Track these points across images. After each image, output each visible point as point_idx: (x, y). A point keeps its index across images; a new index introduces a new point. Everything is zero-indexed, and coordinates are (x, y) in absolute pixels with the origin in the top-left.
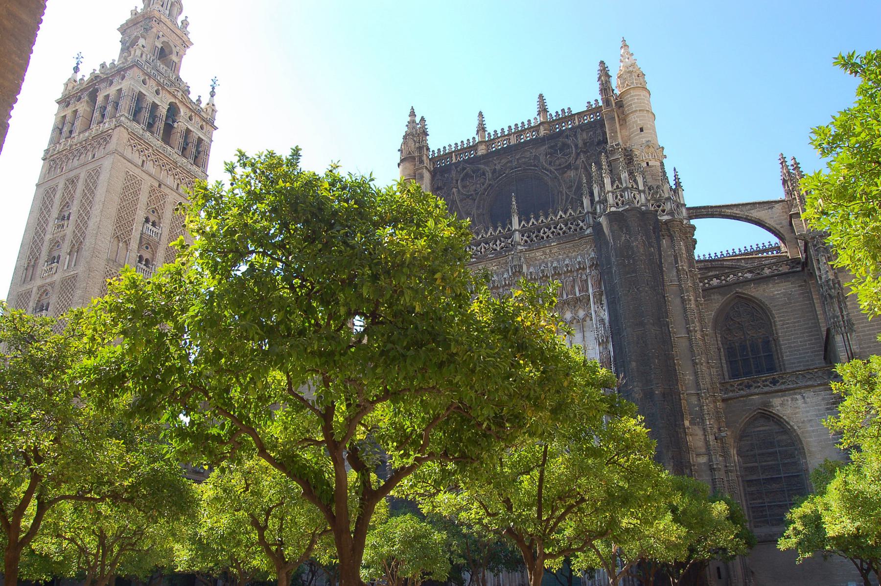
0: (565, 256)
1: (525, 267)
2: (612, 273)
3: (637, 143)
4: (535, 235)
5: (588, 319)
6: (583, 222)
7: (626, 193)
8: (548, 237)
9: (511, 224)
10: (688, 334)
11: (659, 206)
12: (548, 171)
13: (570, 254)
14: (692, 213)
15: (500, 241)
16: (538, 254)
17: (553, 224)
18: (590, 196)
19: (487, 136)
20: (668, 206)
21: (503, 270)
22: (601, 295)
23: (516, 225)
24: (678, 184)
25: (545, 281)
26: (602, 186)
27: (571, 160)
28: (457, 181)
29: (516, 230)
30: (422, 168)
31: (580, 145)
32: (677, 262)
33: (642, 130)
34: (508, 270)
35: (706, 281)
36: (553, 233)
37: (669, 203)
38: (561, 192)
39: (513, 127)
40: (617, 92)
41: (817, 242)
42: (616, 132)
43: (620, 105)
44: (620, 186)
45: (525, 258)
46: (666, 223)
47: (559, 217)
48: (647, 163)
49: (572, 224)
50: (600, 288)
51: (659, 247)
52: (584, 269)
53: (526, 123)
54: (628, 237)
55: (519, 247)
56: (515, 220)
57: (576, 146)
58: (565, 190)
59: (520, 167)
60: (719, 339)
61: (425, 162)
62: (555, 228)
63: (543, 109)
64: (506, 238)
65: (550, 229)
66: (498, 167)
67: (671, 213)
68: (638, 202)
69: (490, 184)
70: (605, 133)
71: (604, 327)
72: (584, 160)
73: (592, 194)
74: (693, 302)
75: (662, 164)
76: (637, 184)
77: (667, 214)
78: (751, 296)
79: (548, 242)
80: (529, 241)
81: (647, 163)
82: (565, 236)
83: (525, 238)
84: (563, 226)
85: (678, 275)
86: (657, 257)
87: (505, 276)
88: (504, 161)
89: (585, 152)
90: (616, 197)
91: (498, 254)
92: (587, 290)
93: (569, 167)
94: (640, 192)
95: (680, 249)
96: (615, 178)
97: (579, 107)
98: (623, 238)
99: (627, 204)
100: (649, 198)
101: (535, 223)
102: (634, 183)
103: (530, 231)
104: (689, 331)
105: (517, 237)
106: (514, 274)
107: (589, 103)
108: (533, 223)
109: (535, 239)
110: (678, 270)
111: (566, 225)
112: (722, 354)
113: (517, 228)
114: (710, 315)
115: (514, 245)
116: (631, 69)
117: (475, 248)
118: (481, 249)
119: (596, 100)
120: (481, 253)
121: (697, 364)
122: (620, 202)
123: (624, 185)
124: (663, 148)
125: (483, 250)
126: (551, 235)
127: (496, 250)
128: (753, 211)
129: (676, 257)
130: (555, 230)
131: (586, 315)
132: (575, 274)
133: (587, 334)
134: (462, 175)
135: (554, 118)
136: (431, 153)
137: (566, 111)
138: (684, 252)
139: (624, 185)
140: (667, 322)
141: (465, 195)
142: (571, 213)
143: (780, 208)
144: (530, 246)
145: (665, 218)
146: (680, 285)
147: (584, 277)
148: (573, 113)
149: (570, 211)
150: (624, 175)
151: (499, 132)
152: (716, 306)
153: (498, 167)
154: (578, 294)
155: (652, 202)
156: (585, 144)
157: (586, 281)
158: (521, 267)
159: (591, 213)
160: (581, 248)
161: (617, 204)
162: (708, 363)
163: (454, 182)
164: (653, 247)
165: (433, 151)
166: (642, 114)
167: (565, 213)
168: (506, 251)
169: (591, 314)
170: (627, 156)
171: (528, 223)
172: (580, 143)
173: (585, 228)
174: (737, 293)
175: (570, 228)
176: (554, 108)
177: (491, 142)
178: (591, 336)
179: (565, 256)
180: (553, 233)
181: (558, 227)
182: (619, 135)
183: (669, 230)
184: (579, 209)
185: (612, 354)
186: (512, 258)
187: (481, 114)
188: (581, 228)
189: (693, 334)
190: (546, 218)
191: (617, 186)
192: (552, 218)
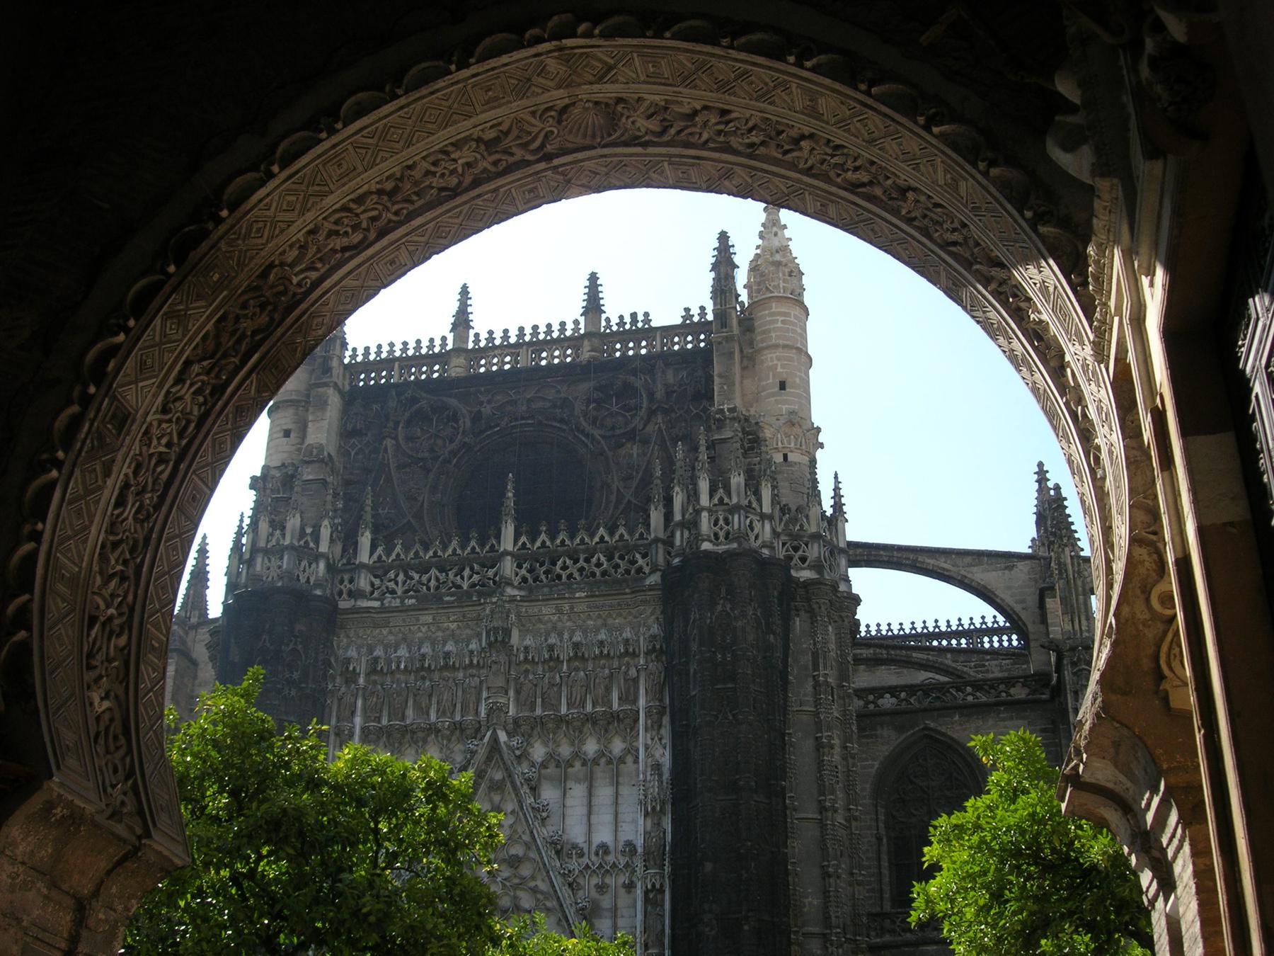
0: (599, 622)
1: (515, 634)
2: (688, 675)
3: (771, 410)
4: (544, 569)
5: (629, 759)
6: (644, 556)
7: (736, 517)
8: (570, 576)
9: (498, 537)
10: (821, 813)
11: (796, 549)
12: (587, 435)
13: (610, 621)
14: (861, 555)
15: (472, 569)
16: (547, 610)
17: (585, 551)
18: (665, 506)
19: (472, 338)
20: (814, 551)
21: (469, 632)
22: (661, 713)
23: (507, 543)
24: (838, 506)
25: (551, 669)
26: (693, 495)
27: (637, 422)
28: (397, 423)
29: (506, 553)
30: (326, 385)
31: (660, 393)
32: (816, 668)
33: (783, 386)
34: (479, 635)
35: (871, 697)
36: (581, 570)
37: (816, 546)
39: (528, 331)
40: (744, 297)
41: (1079, 659)
42: (733, 384)
43: (748, 322)
44: (726, 500)
45: (518, 615)
46: (807, 584)
47: (597, 539)
48: (785, 457)
49: (622, 558)
50: (661, 700)
51: (787, 629)
52: (635, 655)
53: (556, 327)
54: (728, 606)
55: (510, 591)
56: (508, 530)
57: (651, 395)
59: (532, 417)
60: (882, 817)
61: (335, 372)
62: (587, 560)
63: (593, 305)
64: (483, 566)
65: (576, 561)
66: (486, 410)
67: (818, 567)
68: (757, 538)
69: (465, 443)
70: (710, 379)
71: (660, 781)
72: (663, 427)
73: (668, 502)
74: (837, 750)
75: (813, 462)
76: (759, 500)
77: (810, 568)
78: (952, 739)
79: (569, 586)
80: (530, 580)
81: (785, 457)
82: (606, 582)
83: (523, 572)
85: (816, 693)
86: (778, 654)
87: (473, 646)
88: (500, 398)
89: (666, 412)
90: (716, 524)
91: (463, 598)
92: (635, 701)
93: (631, 436)
94: (763, 517)
95: (826, 642)
96: (719, 483)
97: (666, 316)
98: (719, 608)
99: (736, 539)
100: (779, 530)
101: (548, 543)
102: (753, 498)
103: (535, 558)
104: (822, 809)
105: (508, 566)
106: (490, 645)
107: (687, 310)
108: (544, 542)
109: (543, 577)
110: (817, 684)
111: (610, 558)
112: (884, 848)
113: (510, 547)
114: (870, 766)
115: (500, 583)
116: (778, 257)
117: (416, 576)
118: (429, 580)
119: (702, 308)
120: (428, 589)
121: (830, 876)
122: (721, 534)
123: (735, 500)
124: (818, 430)
125: (433, 583)
126: (576, 575)
127: (460, 587)
128: (975, 569)
129: (815, 656)
130: (585, 565)
131: (627, 751)
132: (616, 664)
133: (625, 790)
134: (407, 414)
135: (615, 328)
136: (348, 353)
137: (640, 317)
138: (832, 646)
139: (735, 500)
140: (784, 788)
142: (622, 536)
143: (1026, 570)
144: (531, 590)
145: (806, 575)
146: (817, 714)
147: (633, 672)
148: (653, 324)
149: (622, 530)
150: (737, 480)
151: (498, 336)
152: (884, 750)
153: (486, 410)
154: (615, 706)
155: (783, 538)
156: (669, 394)
157: (636, 681)
158: (507, 632)
159: (664, 542)
161: (716, 535)
162: (852, 874)
163: (391, 424)
164: (774, 633)
165: (354, 350)
166: (786, 354)
167: (612, 534)
168: (480, 594)
169: (637, 750)
170: (748, 433)
171: (533, 541)
172: (660, 393)
173: (647, 570)
174: (926, 728)
175: (617, 566)
176: (615, 309)
177: (479, 353)
178: (630, 795)
179: (599, 622)
180: (581, 570)
181: (594, 560)
182: (737, 388)
183: (808, 600)
184: (641, 529)
185: (669, 838)
186: (492, 611)
187: (464, 292)
188: (639, 570)
189: (829, 814)
190: (572, 538)
191: (721, 500)
192: (582, 540)
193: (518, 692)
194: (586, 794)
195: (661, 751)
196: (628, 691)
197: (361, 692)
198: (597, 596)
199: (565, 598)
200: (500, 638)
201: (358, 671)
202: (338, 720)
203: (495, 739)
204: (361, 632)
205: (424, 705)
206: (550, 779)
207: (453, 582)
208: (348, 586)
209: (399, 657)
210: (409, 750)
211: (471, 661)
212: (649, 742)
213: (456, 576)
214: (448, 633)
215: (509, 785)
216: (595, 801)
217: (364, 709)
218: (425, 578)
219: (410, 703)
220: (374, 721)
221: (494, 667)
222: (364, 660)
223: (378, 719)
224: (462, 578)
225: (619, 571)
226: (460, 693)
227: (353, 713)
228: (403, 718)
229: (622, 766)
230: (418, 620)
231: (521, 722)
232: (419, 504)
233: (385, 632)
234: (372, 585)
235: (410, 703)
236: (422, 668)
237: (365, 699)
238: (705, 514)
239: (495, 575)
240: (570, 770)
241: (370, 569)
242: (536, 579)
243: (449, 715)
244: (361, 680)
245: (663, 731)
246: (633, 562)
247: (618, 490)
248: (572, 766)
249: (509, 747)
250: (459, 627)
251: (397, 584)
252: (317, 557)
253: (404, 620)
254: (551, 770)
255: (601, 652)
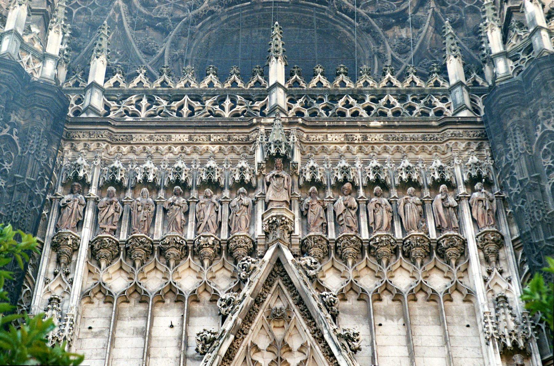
2: (543, 191)
5: (456, 297)
6: (444, 100)
8: (355, 114)
29: (277, 85)
38: (379, 55)
58: (390, 52)
62: (372, 100)
65: (362, 101)
69: (212, 12)
83: (297, 106)
84: (393, 100)
113: (282, 82)
118: (181, 107)
120: (179, 115)
125: (186, 110)
141: (146, 16)
147: (452, 201)
157: (457, 209)
160: (442, 147)
180: (369, 110)
193: (304, 215)
194: (403, 332)
195: (505, 285)
196: (449, 219)
197: (91, 203)
198: (395, 127)
199: (356, 127)
200: (283, 151)
201: (89, 180)
202: (56, 229)
203: (279, 262)
204: (93, 146)
205: (178, 220)
206: (351, 312)
207: (209, 111)
208: (75, 106)
209: (146, 169)
210: (153, 274)
211: (242, 178)
212: (486, 275)
213: (214, 105)
214: (206, 156)
215: (297, 314)
216: (417, 341)
217: (96, 223)
218: (175, 105)
219: (159, 218)
220: (109, 233)
221: (274, 183)
222: (97, 172)
223: (114, 231)
224: (222, 108)
225: (415, 112)
226: (226, 212)
227: (80, 224)
228: (148, 233)
229: (448, 303)
230: (170, 138)
231: (311, 243)
232: (158, 55)
233: (125, 149)
234: (107, 107)
235: (159, 218)
236: (178, 182)
237: (97, 211)
238: (544, 33)
239: (264, 107)
240: (377, 304)
241: (106, 94)
242: (314, 114)
243: (213, 231)
244: (93, 191)
245: (502, 264)
246: (430, 105)
247: (393, 59)
248: (380, 300)
249: (299, 266)
250: (220, 150)
251: (139, 108)
252: (44, 57)
253: (151, 138)
254: (352, 302)
255: (410, 178)
